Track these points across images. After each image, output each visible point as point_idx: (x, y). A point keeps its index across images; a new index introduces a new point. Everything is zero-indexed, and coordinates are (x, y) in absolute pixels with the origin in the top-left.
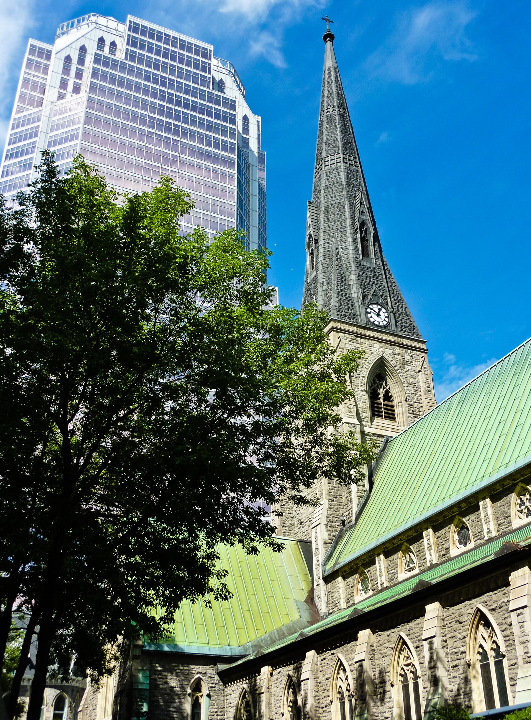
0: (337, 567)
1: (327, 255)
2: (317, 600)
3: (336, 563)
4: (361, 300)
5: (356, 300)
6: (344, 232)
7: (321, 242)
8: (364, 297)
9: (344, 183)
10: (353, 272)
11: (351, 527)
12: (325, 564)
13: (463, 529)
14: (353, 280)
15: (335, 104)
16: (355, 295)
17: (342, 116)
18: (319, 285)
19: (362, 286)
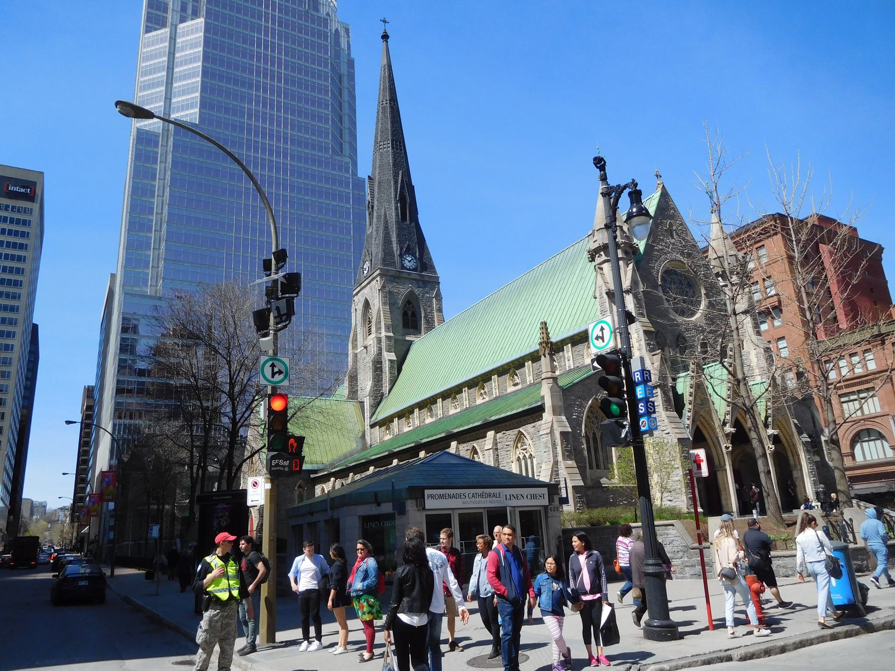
0: (376, 421)
1: (379, 217)
2: (366, 436)
3: (376, 419)
4: (398, 253)
5: (395, 252)
6: (389, 202)
7: (375, 208)
8: (401, 249)
9: (391, 164)
10: (395, 232)
11: (386, 397)
12: (371, 418)
13: (431, 410)
14: (394, 239)
15: (388, 98)
16: (395, 249)
17: (391, 107)
18: (373, 240)
19: (400, 242)
